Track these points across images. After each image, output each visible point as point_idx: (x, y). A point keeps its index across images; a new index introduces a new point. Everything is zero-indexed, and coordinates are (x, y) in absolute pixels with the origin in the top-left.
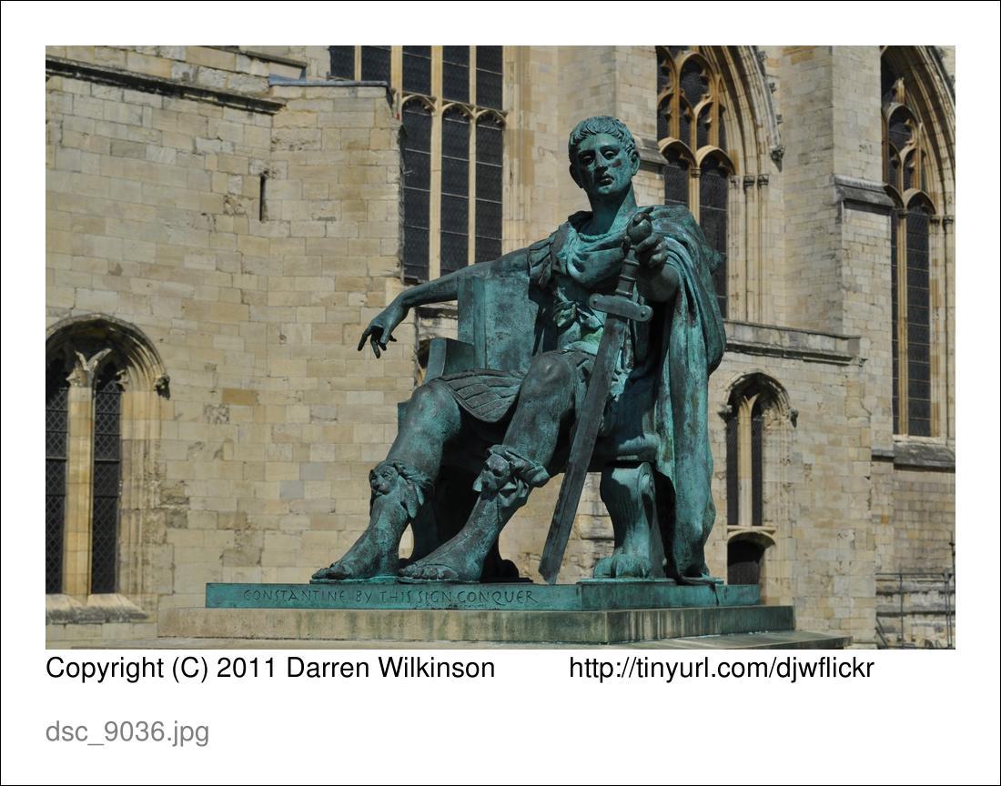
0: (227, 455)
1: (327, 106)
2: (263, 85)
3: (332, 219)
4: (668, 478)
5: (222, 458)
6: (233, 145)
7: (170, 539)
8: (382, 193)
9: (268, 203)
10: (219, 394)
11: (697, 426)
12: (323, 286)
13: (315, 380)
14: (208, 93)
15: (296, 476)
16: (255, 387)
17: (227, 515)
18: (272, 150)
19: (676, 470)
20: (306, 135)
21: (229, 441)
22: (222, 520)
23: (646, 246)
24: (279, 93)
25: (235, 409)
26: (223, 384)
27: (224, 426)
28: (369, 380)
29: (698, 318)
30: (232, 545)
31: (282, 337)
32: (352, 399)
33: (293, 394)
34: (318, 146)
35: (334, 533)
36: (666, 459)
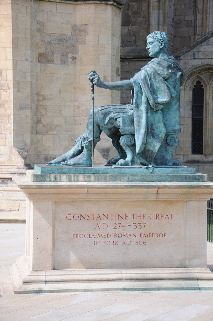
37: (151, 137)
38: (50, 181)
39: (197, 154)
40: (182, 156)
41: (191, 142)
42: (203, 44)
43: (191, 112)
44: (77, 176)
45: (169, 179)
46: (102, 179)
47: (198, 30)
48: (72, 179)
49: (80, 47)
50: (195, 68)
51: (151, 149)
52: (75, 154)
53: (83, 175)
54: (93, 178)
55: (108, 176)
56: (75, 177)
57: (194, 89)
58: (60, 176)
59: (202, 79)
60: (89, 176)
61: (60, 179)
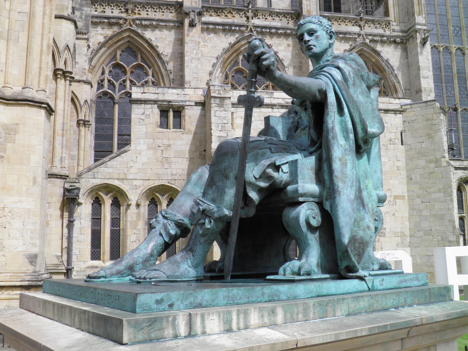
0: (396, 215)
1: (419, 109)
2: (400, 106)
3: (423, 142)
4: (327, 211)
5: (395, 216)
6: (391, 124)
7: (380, 240)
8: (438, 132)
9: (403, 140)
10: (393, 197)
11: (346, 177)
12: (422, 162)
13: (422, 191)
14: (382, 110)
15: (418, 220)
16: (404, 194)
17: (398, 233)
18: (403, 124)
19: (331, 207)
20: (412, 119)
21: (397, 211)
22: (396, 234)
23: (255, 55)
24: (404, 107)
25: (398, 201)
26: (393, 194)
27: (395, 207)
28: (439, 190)
29: (346, 110)
30: (400, 241)
31: (411, 179)
32: (434, 196)
33: (415, 195)
34: (417, 121)
35: (431, 237)
36: (327, 199)
37: (361, 208)
38: (176, 337)
39: (96, 260)
40: (83, 262)
41: (90, 249)
42: (101, 166)
43: (90, 224)
44: (246, 314)
45: (409, 301)
46: (300, 316)
47: (81, 162)
48: (234, 327)
49: (9, 145)
50: (95, 186)
51: (361, 233)
52: (155, 252)
53: (260, 308)
54: (280, 318)
55: (311, 304)
56: (242, 316)
57: (93, 204)
58: (203, 316)
59: (100, 195)
60: (273, 312)
61: (204, 327)
